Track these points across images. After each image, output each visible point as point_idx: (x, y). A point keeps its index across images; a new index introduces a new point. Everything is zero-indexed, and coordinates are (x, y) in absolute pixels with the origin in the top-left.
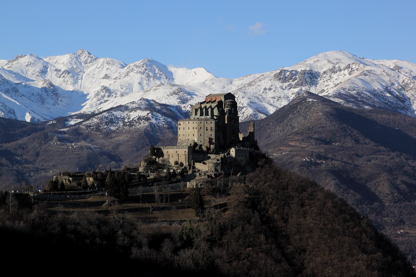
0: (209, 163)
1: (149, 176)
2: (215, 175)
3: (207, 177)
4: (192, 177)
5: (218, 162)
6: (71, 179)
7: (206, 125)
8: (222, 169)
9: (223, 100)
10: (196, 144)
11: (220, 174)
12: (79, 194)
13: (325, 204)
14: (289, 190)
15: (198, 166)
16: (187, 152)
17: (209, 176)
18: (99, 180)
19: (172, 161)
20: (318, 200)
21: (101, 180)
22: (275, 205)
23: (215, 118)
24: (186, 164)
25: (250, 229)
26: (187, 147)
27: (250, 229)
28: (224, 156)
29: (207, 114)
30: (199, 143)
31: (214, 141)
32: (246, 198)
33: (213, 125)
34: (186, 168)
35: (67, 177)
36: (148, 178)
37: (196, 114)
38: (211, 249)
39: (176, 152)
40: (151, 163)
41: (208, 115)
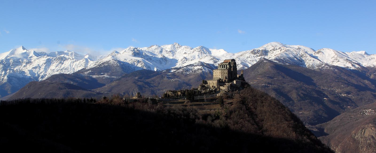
0: (226, 86)
1: (202, 92)
2: (228, 91)
4: (219, 92)
5: (229, 86)
6: (172, 93)
8: (230, 89)
9: (231, 62)
10: (220, 79)
11: (230, 91)
12: (175, 99)
13: (271, 102)
14: (257, 97)
15: (221, 87)
17: (225, 92)
18: (183, 93)
19: (211, 86)
20: (268, 100)
21: (183, 94)
22: (251, 103)
23: (228, 69)
24: (216, 87)
25: (242, 112)
27: (242, 112)
28: (231, 84)
29: (224, 67)
30: (221, 79)
31: (227, 78)
32: (240, 100)
33: (227, 72)
34: (216, 88)
35: (170, 92)
36: (202, 92)
37: (220, 67)
38: (226, 120)
40: (203, 87)
41: (225, 68)
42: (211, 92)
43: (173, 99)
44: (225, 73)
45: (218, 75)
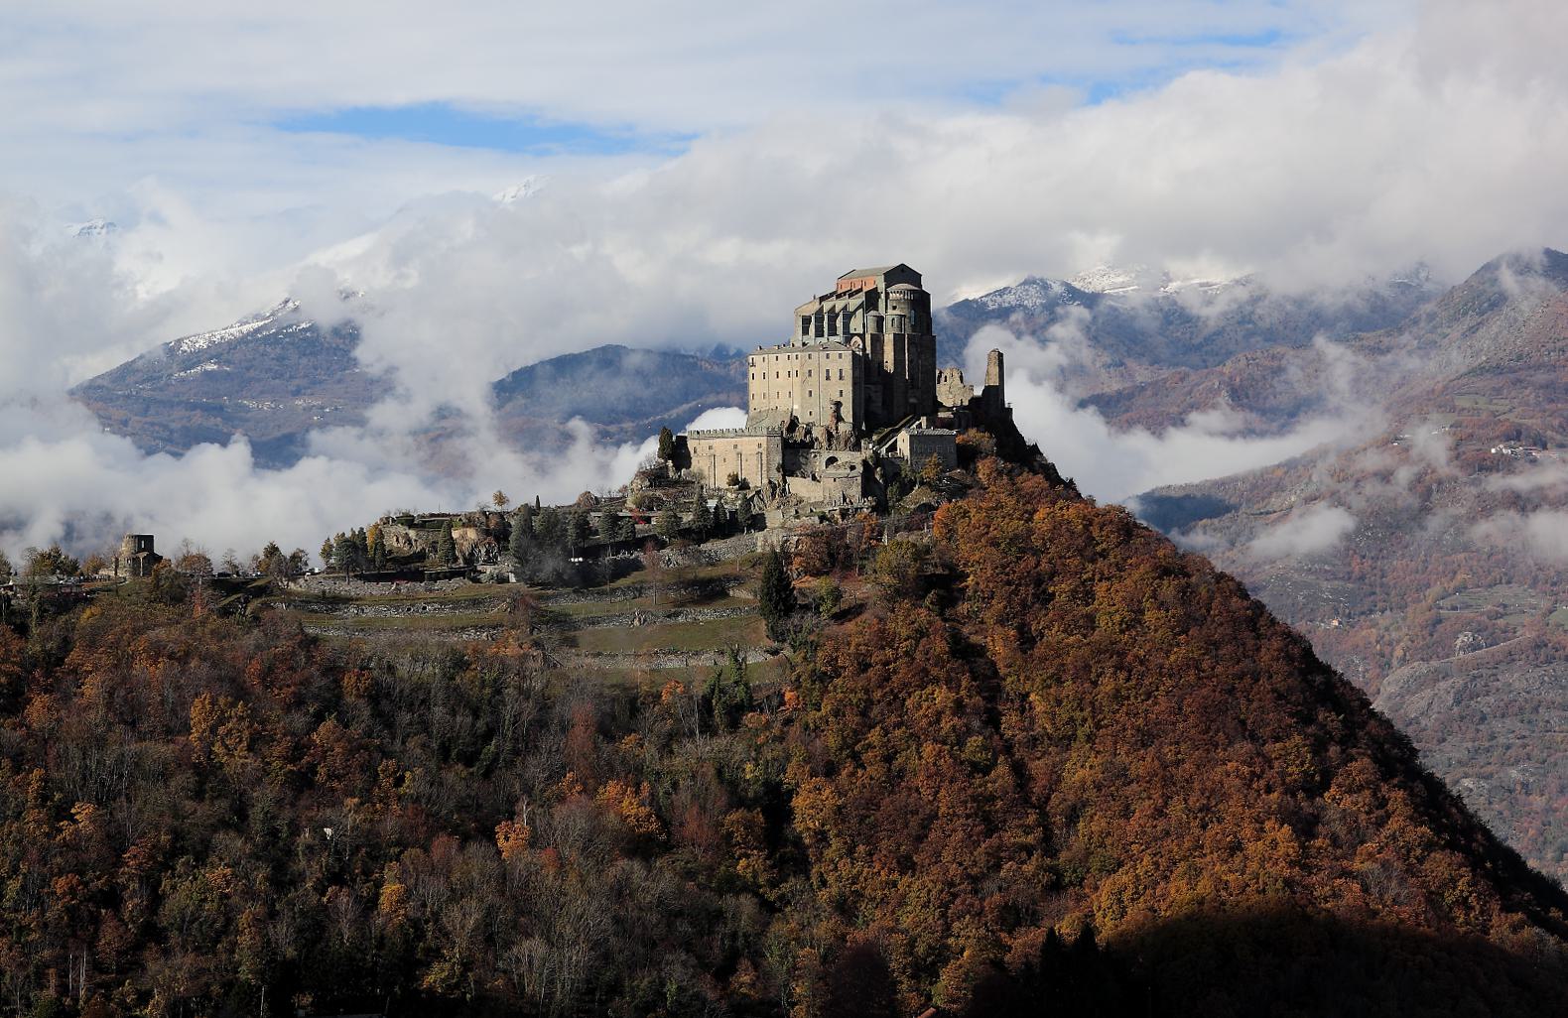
3: (816, 519)
7: (826, 364)
10: (793, 424)
15: (797, 485)
16: (764, 445)
17: (823, 518)
26: (765, 432)
29: (833, 332)
30: (803, 420)
31: (847, 412)
33: (846, 364)
35: (401, 529)
37: (805, 331)
39: (736, 447)
41: (836, 334)
44: (835, 375)
45: (784, 394)
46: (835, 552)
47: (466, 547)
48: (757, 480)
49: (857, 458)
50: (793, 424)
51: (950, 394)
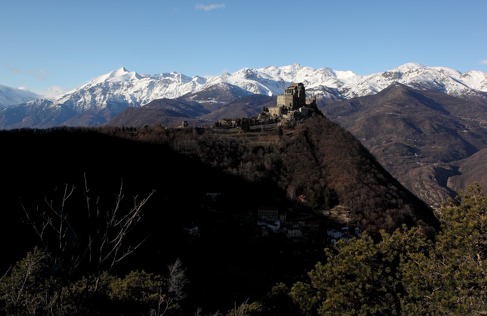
2: (291, 120)
4: (280, 121)
6: (226, 121)
8: (294, 117)
10: (284, 106)
12: (227, 128)
14: (323, 127)
15: (284, 116)
17: (288, 121)
23: (294, 94)
24: (278, 115)
25: (300, 145)
28: (296, 112)
31: (292, 105)
32: (303, 131)
34: (278, 117)
35: (224, 121)
37: (286, 93)
38: (281, 153)
42: (271, 122)
43: (226, 128)
46: (290, 125)
47: (234, 124)
48: (278, 115)
49: (293, 112)
50: (284, 106)
51: (308, 103)
